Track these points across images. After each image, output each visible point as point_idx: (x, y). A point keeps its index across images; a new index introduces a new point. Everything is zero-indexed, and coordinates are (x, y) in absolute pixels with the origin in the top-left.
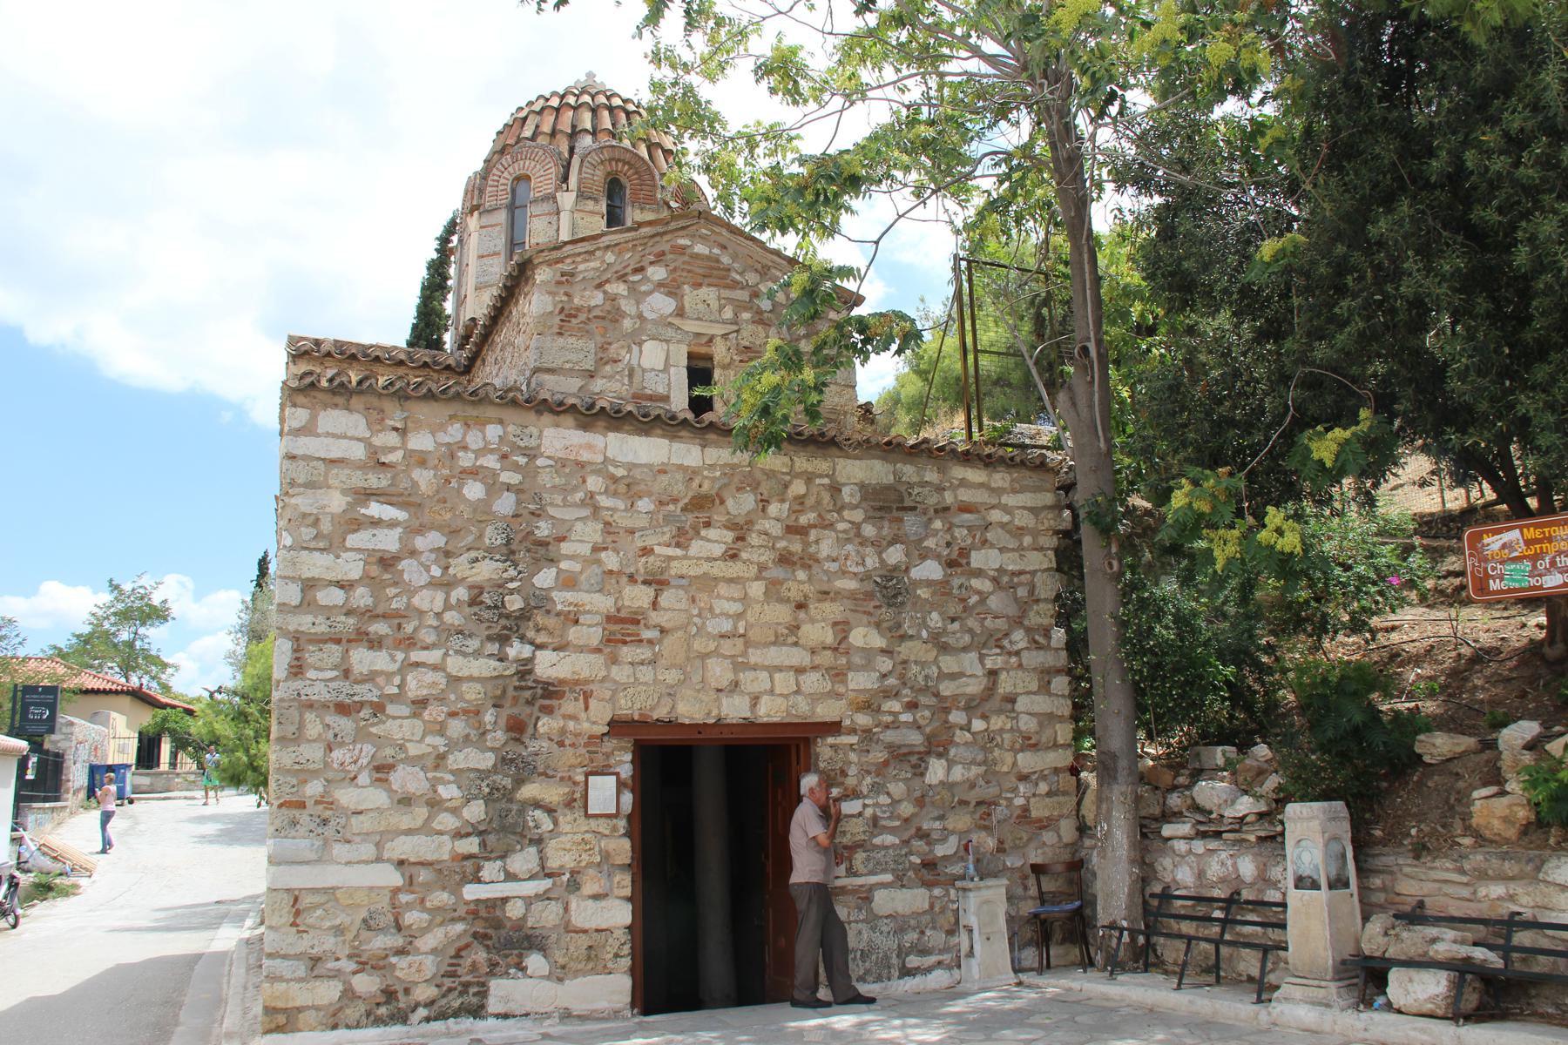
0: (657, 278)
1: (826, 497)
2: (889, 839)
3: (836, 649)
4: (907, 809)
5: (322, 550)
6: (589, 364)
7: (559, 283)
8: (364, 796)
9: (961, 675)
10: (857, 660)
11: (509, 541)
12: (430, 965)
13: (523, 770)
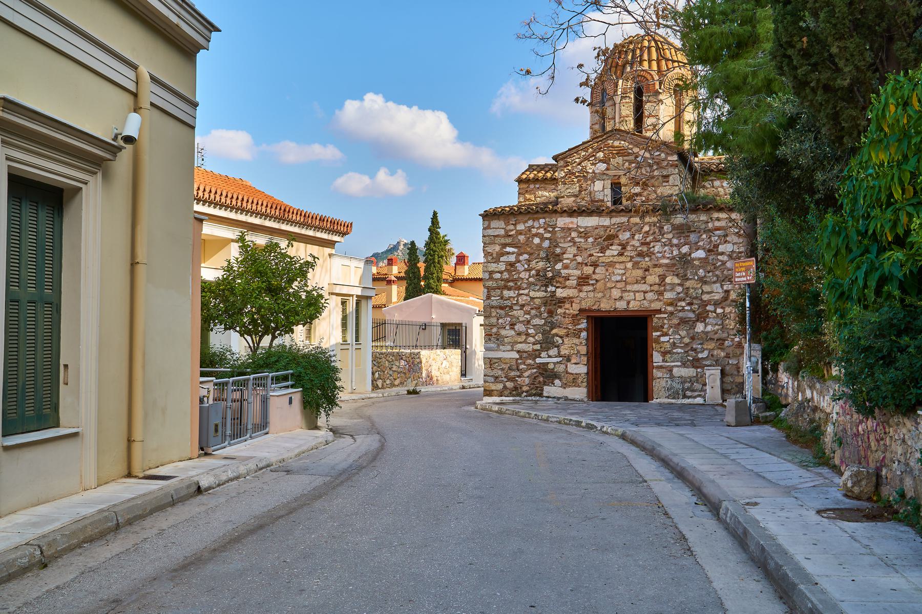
2: (679, 350)
3: (659, 285)
4: (687, 340)
8: (507, 332)
10: (668, 287)
12: (527, 381)
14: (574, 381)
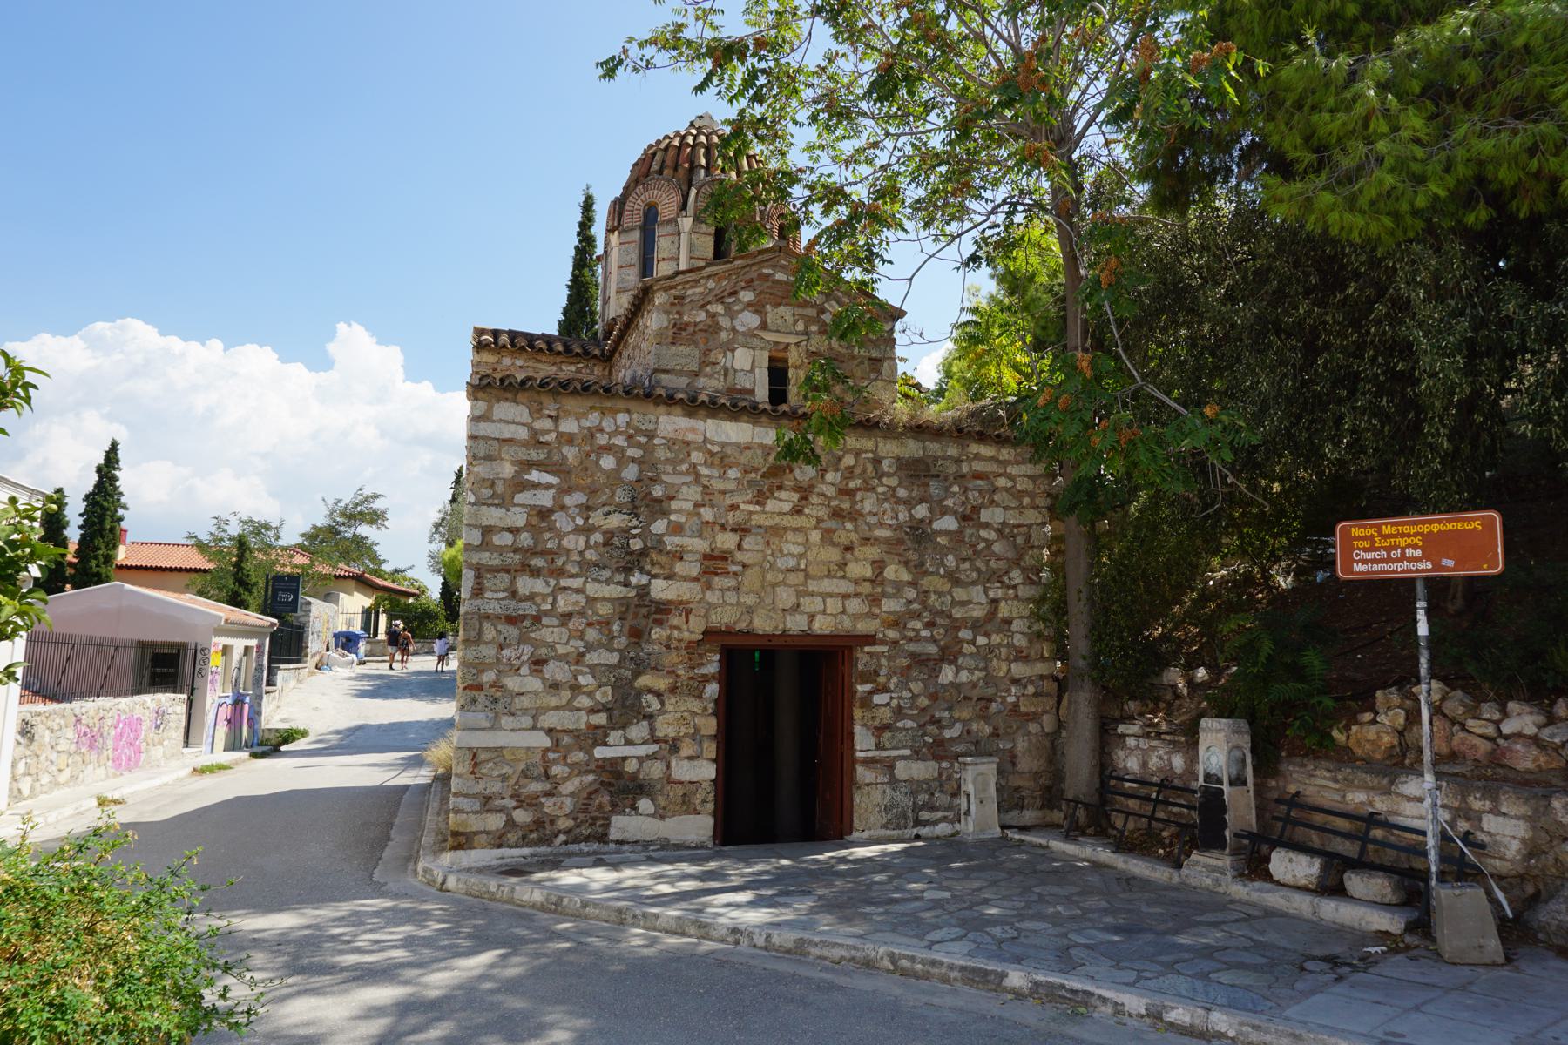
0: (746, 300)
1: (870, 468)
2: (909, 724)
3: (872, 581)
4: (924, 702)
5: (496, 506)
6: (694, 367)
7: (673, 304)
9: (970, 602)
10: (889, 590)
11: (633, 500)
12: (568, 804)
13: (640, 667)
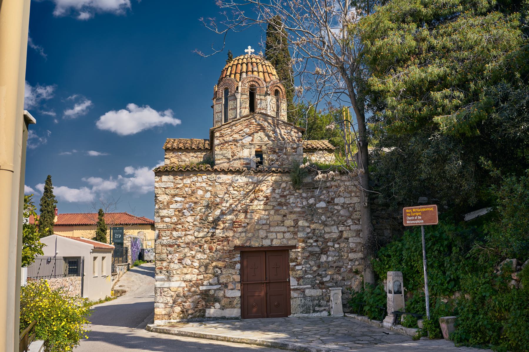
2: (310, 276)
4: (315, 268)
14: (230, 304)
